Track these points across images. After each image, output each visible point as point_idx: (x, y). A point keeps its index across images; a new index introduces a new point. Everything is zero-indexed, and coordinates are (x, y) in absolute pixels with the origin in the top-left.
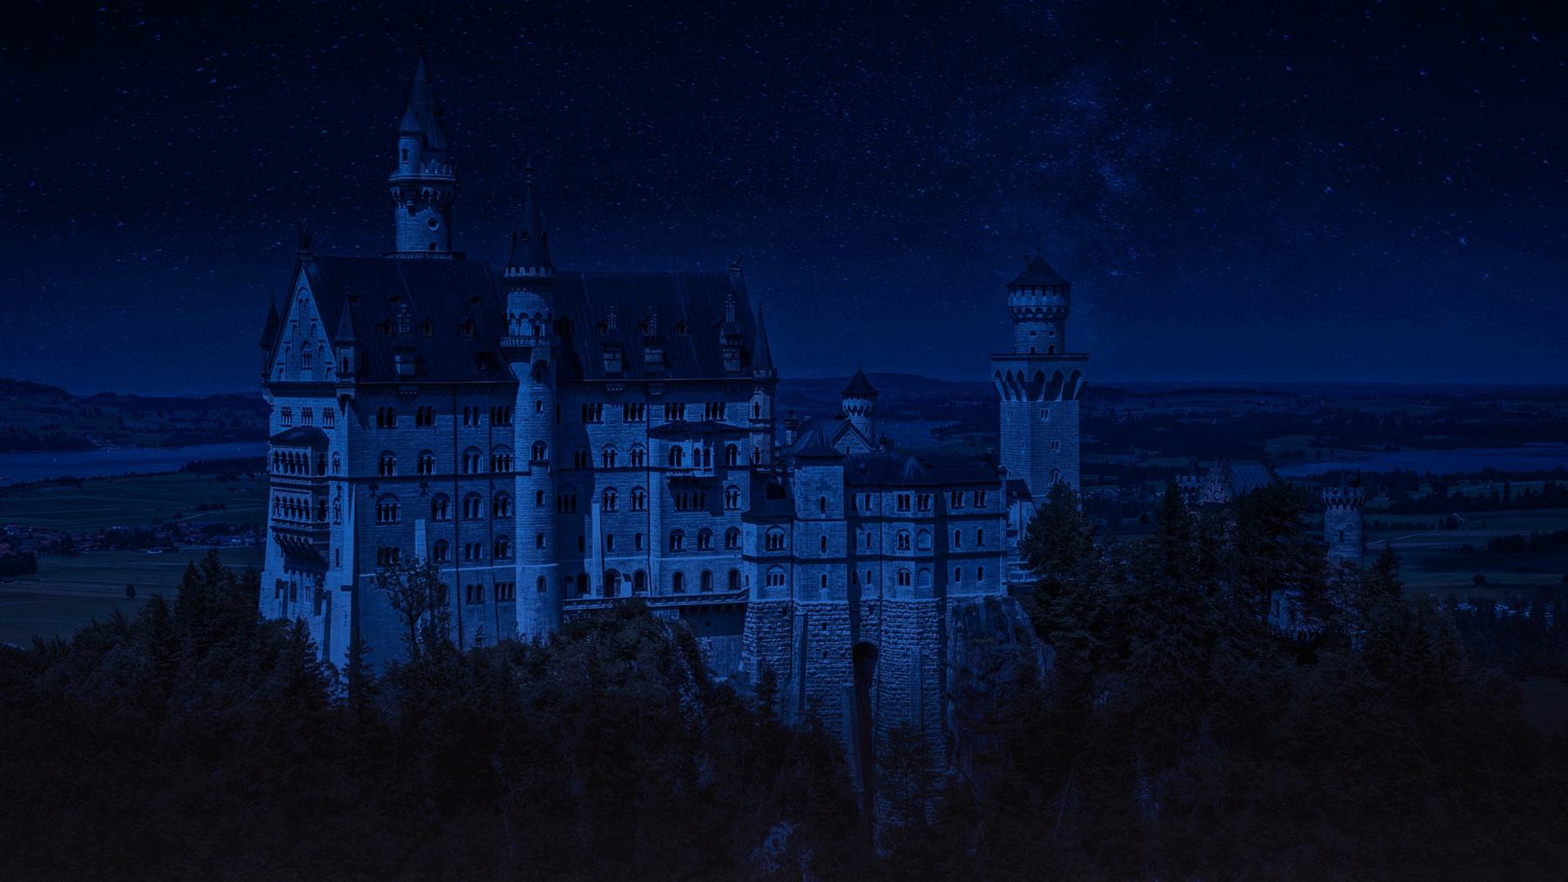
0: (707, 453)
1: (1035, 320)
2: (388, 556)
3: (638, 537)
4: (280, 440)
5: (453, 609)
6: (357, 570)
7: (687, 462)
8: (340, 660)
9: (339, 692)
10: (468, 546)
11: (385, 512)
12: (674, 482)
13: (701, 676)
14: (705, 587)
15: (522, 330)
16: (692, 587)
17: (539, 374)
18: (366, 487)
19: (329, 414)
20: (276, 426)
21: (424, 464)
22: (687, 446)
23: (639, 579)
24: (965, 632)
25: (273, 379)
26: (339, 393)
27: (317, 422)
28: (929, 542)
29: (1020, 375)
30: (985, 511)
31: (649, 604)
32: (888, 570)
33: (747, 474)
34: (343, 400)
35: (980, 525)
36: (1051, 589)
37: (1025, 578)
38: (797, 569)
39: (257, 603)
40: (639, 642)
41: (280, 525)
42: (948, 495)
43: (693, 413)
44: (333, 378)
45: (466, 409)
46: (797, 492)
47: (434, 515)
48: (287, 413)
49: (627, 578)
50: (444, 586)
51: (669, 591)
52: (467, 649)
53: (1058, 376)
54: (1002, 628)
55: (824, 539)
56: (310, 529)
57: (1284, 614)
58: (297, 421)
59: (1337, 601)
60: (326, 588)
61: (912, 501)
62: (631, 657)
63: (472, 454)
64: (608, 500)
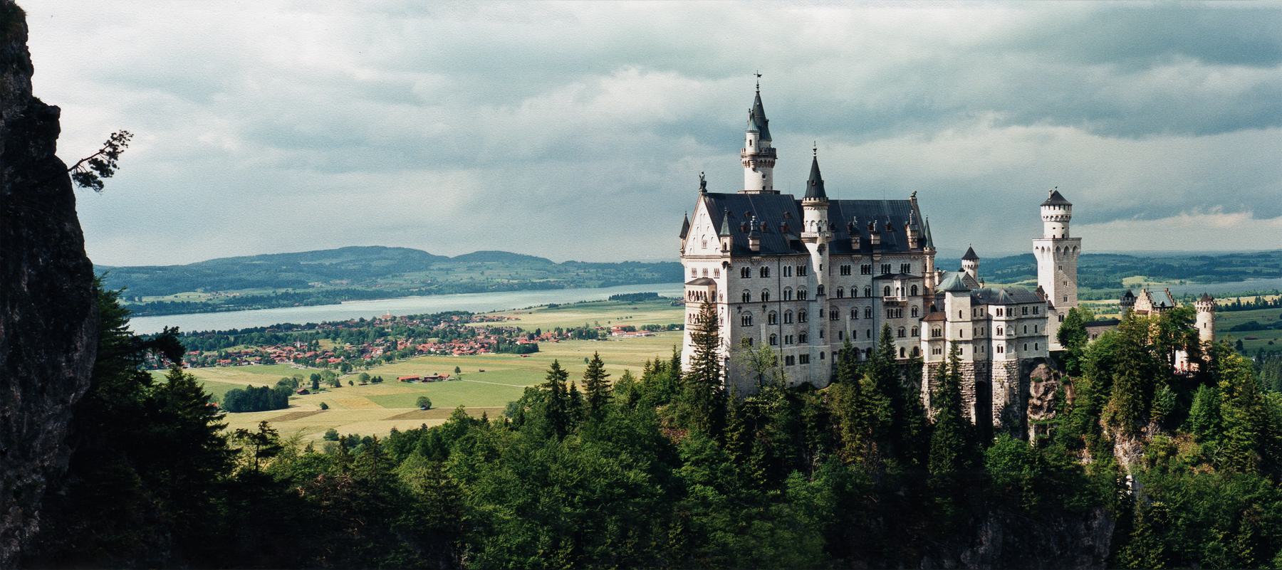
7: (893, 294)
11: (747, 321)
15: (810, 230)
17: (821, 250)
19: (717, 272)
20: (688, 277)
21: (765, 296)
27: (711, 275)
34: (725, 264)
35: (1036, 322)
43: (896, 269)
46: (948, 308)
48: (694, 272)
53: (1067, 248)
58: (700, 275)
64: (854, 314)
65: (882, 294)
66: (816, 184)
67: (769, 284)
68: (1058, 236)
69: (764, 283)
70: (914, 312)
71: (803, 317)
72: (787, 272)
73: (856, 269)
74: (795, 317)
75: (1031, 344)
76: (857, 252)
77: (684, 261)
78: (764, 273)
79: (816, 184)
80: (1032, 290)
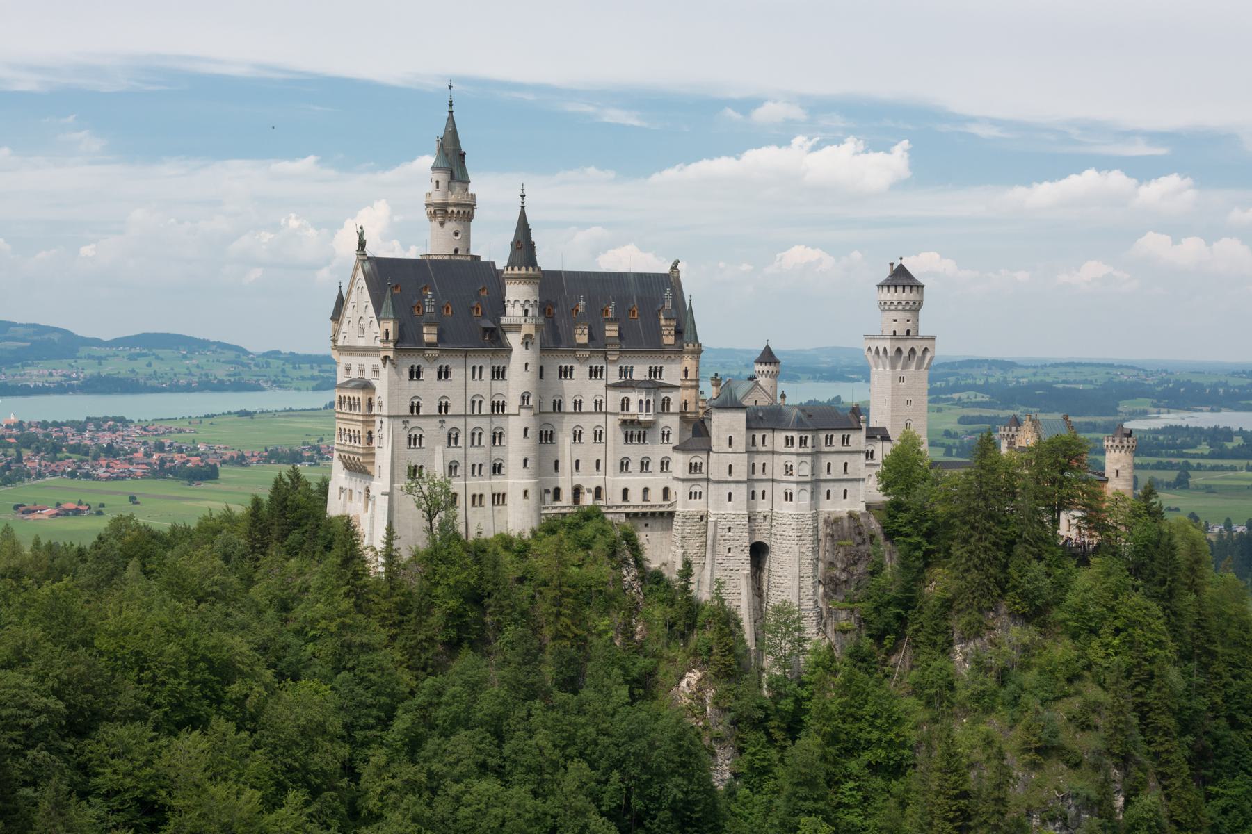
0: (648, 402)
1: (896, 310)
2: (414, 472)
3: (598, 462)
4: (343, 386)
5: (460, 511)
6: (392, 482)
7: (634, 408)
8: (380, 545)
9: (377, 567)
10: (474, 466)
11: (415, 441)
12: (624, 423)
13: (639, 563)
14: (645, 499)
15: (514, 312)
18: (401, 421)
19: (376, 370)
20: (341, 378)
21: (443, 407)
22: (635, 397)
23: (598, 492)
24: (832, 536)
25: (340, 343)
26: (383, 354)
27: (368, 375)
28: (807, 469)
29: (885, 350)
30: (848, 449)
31: (604, 510)
32: (780, 490)
33: (676, 419)
34: (386, 358)
35: (846, 458)
36: (897, 507)
37: (879, 497)
38: (711, 486)
39: (326, 501)
40: (595, 537)
41: (341, 448)
42: (822, 436)
43: (640, 372)
44: (379, 345)
45: (474, 368)
46: (714, 432)
47: (450, 443)
48: (348, 369)
49: (589, 491)
50: (455, 494)
51: (618, 500)
52: (471, 539)
53: (912, 350)
54: (860, 534)
55: (730, 467)
56: (361, 451)
57: (1068, 526)
58: (355, 374)
59: (1110, 521)
60: (371, 494)
61: (796, 440)
62: (588, 547)
63: (477, 400)
64: (577, 436)
65: (619, 410)
66: (524, 247)
68: (901, 332)
69: (443, 387)
70: (666, 436)
71: (497, 437)
72: (477, 372)
73: (581, 371)
74: (486, 439)
75: (837, 490)
77: (335, 355)
78: (443, 374)
79: (524, 247)
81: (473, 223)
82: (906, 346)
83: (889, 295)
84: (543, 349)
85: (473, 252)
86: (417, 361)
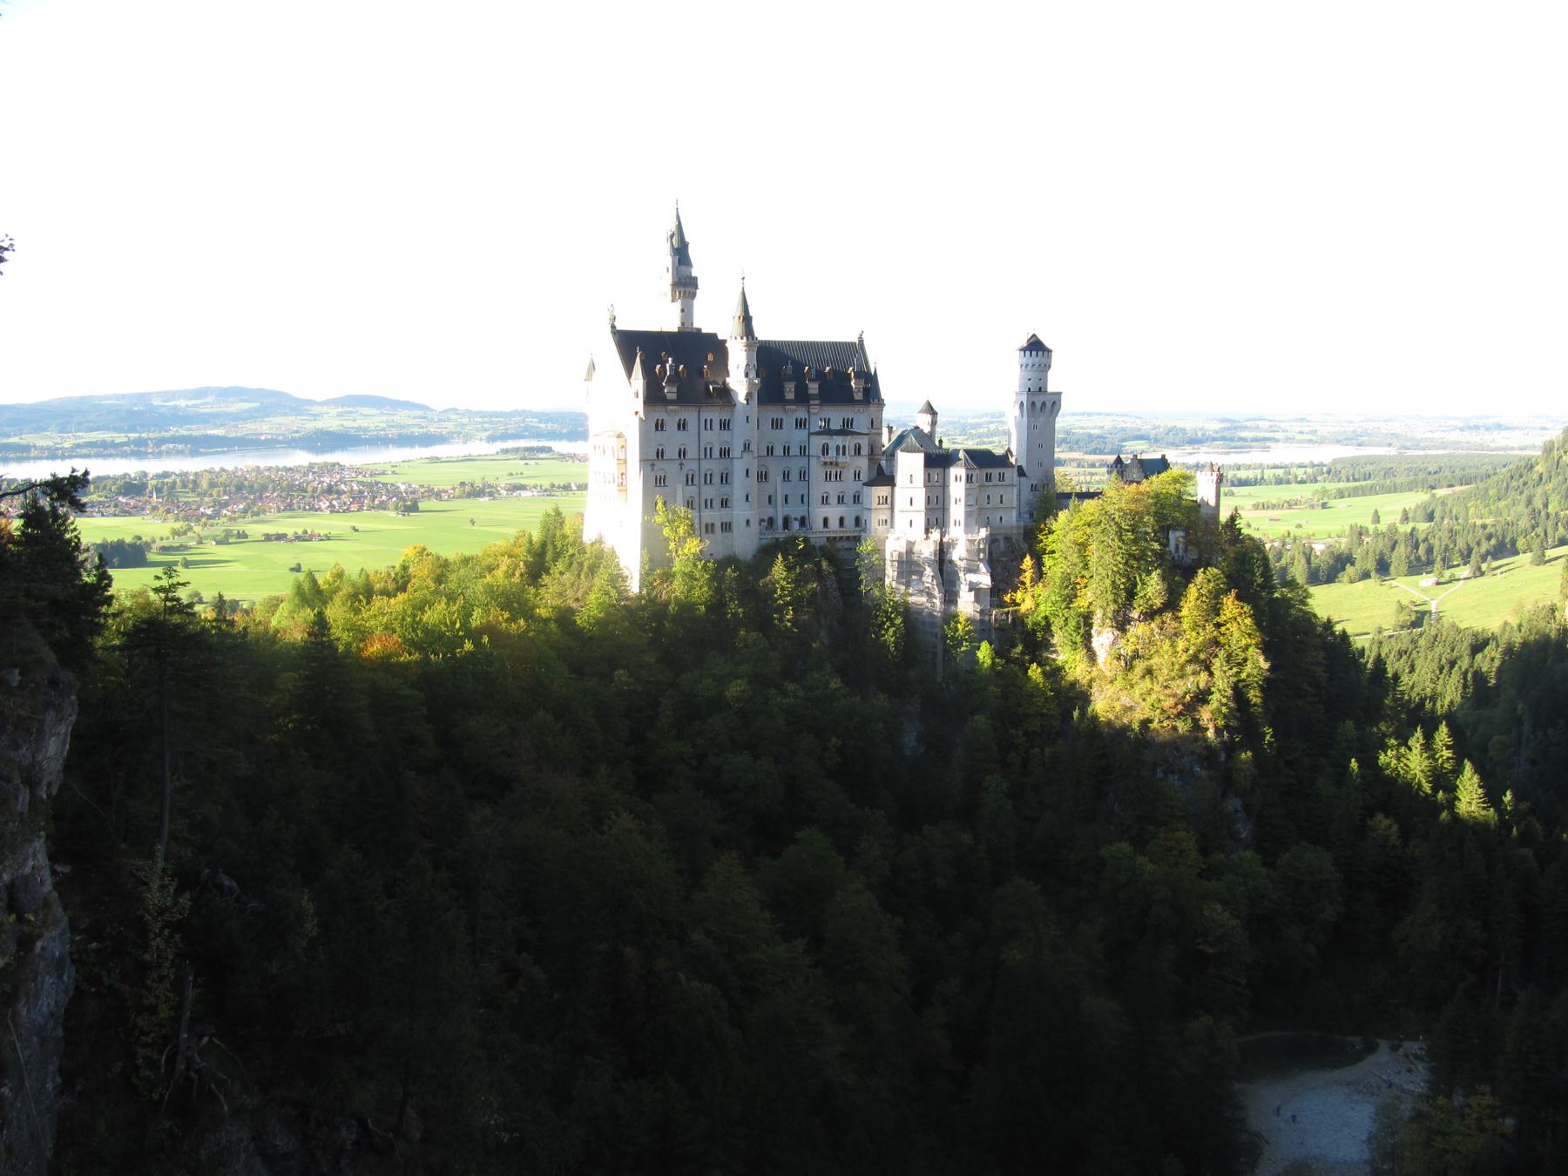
7: (832, 452)
9: (634, 587)
16: (834, 524)
21: (682, 453)
23: (803, 521)
28: (972, 502)
43: (835, 426)
53: (1044, 404)
64: (786, 476)
67: (688, 439)
71: (725, 478)
72: (709, 425)
73: (789, 422)
74: (716, 479)
76: (790, 402)
78: (682, 426)
80: (999, 451)
81: (696, 302)
82: (1039, 400)
83: (1028, 360)
84: (760, 402)
85: (696, 325)
86: (660, 414)
